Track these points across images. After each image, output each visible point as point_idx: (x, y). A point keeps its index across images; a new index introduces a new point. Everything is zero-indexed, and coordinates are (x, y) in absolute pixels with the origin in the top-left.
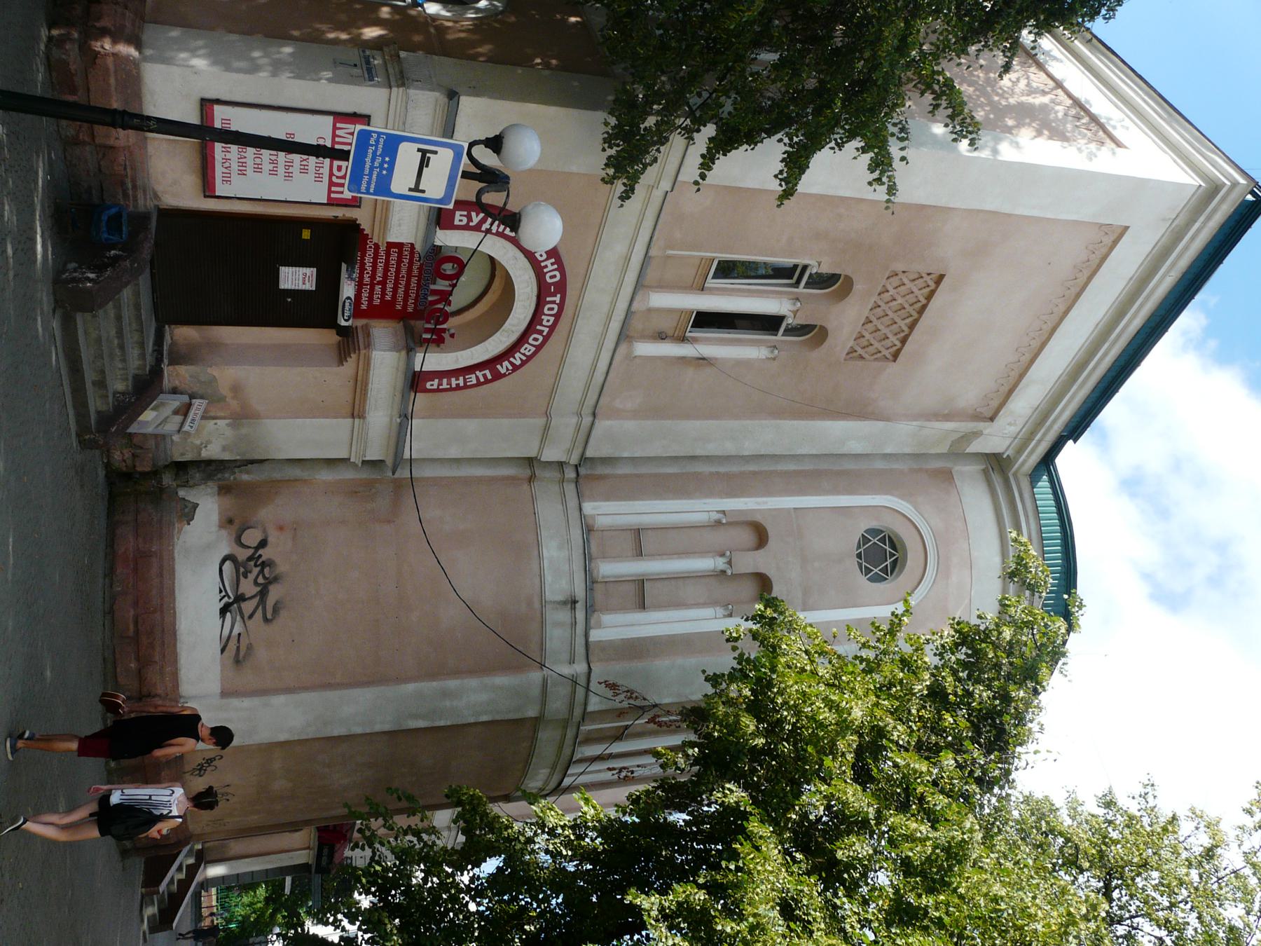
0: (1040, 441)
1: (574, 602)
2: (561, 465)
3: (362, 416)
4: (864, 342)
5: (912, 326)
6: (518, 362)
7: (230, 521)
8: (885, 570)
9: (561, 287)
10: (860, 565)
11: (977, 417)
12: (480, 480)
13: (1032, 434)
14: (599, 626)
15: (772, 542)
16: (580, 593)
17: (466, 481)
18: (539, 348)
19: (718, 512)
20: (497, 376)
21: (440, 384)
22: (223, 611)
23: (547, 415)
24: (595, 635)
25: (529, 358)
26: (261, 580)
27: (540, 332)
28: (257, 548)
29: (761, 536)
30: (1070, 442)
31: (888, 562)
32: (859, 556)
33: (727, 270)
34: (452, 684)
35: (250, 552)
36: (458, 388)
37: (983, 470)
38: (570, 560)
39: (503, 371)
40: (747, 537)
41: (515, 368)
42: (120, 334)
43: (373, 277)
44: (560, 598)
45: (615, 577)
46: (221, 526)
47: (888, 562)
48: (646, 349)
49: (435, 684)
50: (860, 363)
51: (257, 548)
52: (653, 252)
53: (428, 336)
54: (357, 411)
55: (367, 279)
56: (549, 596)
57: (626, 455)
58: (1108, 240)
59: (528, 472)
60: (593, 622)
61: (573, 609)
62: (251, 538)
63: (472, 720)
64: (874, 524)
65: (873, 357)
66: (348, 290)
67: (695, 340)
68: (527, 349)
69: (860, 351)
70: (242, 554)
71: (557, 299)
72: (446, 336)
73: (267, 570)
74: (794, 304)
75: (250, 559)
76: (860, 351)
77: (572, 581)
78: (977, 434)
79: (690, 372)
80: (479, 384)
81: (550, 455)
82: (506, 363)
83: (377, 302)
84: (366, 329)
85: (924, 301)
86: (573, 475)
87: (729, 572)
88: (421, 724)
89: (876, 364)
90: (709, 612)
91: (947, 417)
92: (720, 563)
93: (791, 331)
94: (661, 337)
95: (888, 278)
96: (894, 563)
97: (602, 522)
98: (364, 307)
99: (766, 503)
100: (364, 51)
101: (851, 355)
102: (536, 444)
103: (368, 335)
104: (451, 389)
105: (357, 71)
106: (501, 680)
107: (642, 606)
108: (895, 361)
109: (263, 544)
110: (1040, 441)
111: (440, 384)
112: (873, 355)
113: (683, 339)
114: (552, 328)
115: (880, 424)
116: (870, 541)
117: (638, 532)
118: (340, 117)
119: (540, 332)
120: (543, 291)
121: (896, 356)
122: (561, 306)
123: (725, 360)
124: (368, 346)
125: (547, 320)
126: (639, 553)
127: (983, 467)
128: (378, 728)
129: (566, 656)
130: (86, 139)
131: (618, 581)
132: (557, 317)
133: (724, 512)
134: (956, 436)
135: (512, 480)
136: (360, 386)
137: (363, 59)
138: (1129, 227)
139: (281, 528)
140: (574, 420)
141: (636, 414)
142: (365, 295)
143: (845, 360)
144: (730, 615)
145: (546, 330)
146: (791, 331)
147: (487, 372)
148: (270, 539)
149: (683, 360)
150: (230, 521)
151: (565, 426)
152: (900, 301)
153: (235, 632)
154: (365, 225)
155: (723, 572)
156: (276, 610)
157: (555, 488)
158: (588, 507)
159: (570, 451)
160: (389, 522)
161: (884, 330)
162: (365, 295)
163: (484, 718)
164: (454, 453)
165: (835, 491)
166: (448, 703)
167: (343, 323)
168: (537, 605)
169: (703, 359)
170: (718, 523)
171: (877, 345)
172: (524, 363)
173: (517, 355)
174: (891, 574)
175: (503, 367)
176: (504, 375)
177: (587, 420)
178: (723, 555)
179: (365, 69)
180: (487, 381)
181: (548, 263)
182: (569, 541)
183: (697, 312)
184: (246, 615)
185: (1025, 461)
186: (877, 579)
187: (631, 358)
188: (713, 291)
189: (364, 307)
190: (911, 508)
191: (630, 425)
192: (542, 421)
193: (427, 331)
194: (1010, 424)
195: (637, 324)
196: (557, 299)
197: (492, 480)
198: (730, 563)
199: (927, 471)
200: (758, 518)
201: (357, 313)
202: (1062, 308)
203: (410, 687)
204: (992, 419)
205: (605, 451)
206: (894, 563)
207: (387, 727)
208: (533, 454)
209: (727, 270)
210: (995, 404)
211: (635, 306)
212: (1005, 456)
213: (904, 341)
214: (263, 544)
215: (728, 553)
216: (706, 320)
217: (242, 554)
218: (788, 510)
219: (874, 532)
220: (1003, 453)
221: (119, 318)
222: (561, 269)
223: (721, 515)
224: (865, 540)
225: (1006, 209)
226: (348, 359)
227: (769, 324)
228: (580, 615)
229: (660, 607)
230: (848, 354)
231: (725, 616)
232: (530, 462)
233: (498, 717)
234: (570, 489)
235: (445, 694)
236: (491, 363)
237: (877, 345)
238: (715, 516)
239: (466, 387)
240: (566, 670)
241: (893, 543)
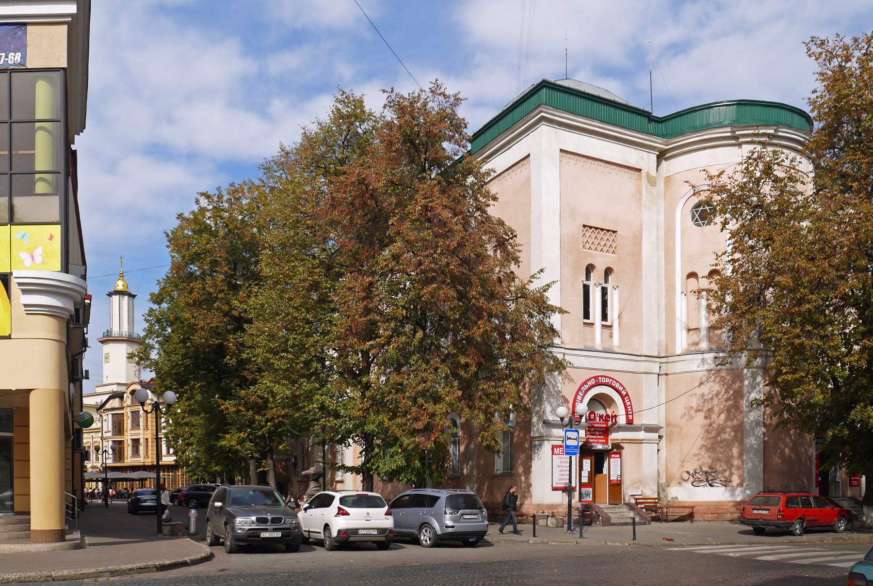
3: (642, 440)
5: (602, 230)
6: (622, 388)
7: (680, 483)
9: (596, 378)
18: (617, 382)
20: (627, 395)
21: (630, 414)
22: (711, 486)
25: (620, 384)
26: (701, 473)
27: (611, 382)
28: (690, 474)
29: (692, 275)
33: (586, 315)
35: (691, 477)
36: (631, 408)
39: (625, 393)
40: (692, 280)
41: (624, 389)
42: (616, 513)
43: (595, 439)
46: (682, 486)
47: (707, 208)
48: (616, 340)
50: (618, 247)
51: (690, 474)
52: (582, 347)
53: (614, 421)
54: (640, 442)
55: (596, 441)
62: (686, 476)
66: (600, 447)
68: (617, 385)
70: (691, 479)
71: (600, 378)
72: (613, 414)
73: (697, 471)
75: (693, 477)
78: (648, 174)
79: (624, 320)
80: (630, 401)
82: (623, 392)
83: (602, 437)
89: (618, 240)
91: (641, 194)
93: (606, 281)
94: (611, 336)
98: (605, 441)
103: (614, 440)
104: (632, 411)
108: (616, 232)
109: (688, 472)
111: (630, 414)
113: (611, 327)
114: (610, 378)
115: (644, 227)
118: (553, 453)
119: (611, 382)
120: (598, 384)
121: (614, 232)
122: (602, 376)
123: (620, 308)
125: (607, 380)
132: (606, 377)
133: (682, 292)
134: (649, 185)
139: (683, 466)
142: (601, 441)
145: (611, 380)
146: (606, 281)
147: (626, 399)
148: (687, 470)
149: (619, 324)
150: (680, 483)
151: (643, 366)
153: (720, 482)
156: (713, 469)
158: (678, 352)
160: (681, 429)
162: (601, 441)
165: (674, 239)
167: (610, 448)
170: (685, 295)
172: (622, 386)
173: (619, 389)
175: (624, 393)
176: (627, 392)
177: (643, 358)
180: (629, 398)
181: (589, 384)
182: (690, 360)
183: (602, 320)
184: (713, 478)
187: (619, 347)
188: (594, 319)
189: (605, 441)
193: (612, 421)
195: (607, 346)
196: (600, 378)
199: (665, 191)
201: (607, 443)
204: (640, 170)
209: (586, 315)
211: (601, 349)
212: (658, 153)
214: (688, 472)
216: (604, 317)
217: (691, 479)
218: (682, 262)
219: (693, 217)
222: (590, 379)
223: (683, 294)
227: (604, 291)
234: (670, 359)
236: (623, 398)
239: (631, 405)
241: (698, 206)
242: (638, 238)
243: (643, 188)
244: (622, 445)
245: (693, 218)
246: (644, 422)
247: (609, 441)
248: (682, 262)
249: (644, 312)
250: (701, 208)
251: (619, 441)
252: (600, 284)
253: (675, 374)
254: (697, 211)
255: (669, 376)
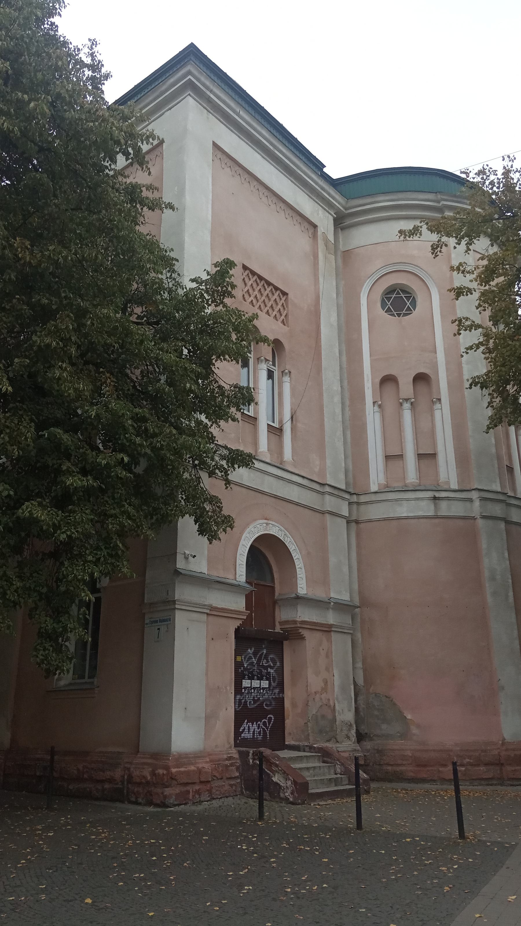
0: (329, 194)
1: (435, 498)
2: (350, 504)
3: (331, 626)
4: (278, 315)
5: (269, 284)
8: (408, 298)
10: (405, 315)
11: (315, 236)
12: (359, 554)
13: (323, 199)
14: (448, 483)
15: (393, 373)
16: (430, 494)
17: (359, 562)
19: (374, 406)
23: (323, 513)
24: (454, 485)
30: (325, 170)
31: (403, 296)
32: (399, 315)
34: (486, 574)
37: (341, 229)
38: (408, 500)
40: (389, 388)
44: (432, 507)
45: (417, 472)
47: (403, 296)
48: (288, 454)
49: (487, 585)
56: (431, 513)
57: (343, 465)
58: (220, 155)
59: (353, 524)
60: (446, 487)
61: (439, 499)
63: (508, 562)
64: (379, 305)
65: (286, 309)
67: (281, 422)
69: (283, 317)
74: (262, 361)
76: (283, 317)
77: (422, 499)
81: (345, 512)
84: (281, 623)
85: (256, 277)
86: (355, 496)
87: (413, 400)
88: (511, 594)
89: (290, 306)
90: (437, 414)
91: (316, 257)
92: (407, 405)
95: (245, 301)
96: (404, 291)
97: (382, 480)
99: (368, 375)
100: (147, 624)
101: (285, 322)
102: (339, 520)
103: (287, 622)
105: (163, 629)
106: (484, 544)
107: (433, 456)
108: (287, 294)
110: (329, 194)
112: (284, 309)
116: (389, 307)
117: (388, 458)
121: (285, 294)
123: (292, 404)
124: (295, 622)
126: (401, 457)
127: (340, 230)
128: (514, 620)
129: (468, 504)
130: (209, 786)
131: (419, 470)
133: (374, 403)
135: (358, 535)
136: (315, 627)
137: (154, 624)
138: (213, 142)
140: (327, 497)
141: (323, 458)
143: (288, 327)
144: (439, 400)
149: (293, 429)
152: (256, 292)
154: (238, 623)
155: (412, 404)
157: (362, 508)
158: (374, 488)
159: (343, 499)
161: (272, 302)
163: (506, 555)
164: (346, 569)
166: (498, 577)
168: (437, 521)
169: (292, 418)
170: (380, 406)
171: (279, 306)
174: (411, 294)
177: (327, 489)
178: (401, 404)
179: (161, 624)
182: (396, 500)
185: (339, 203)
186: (414, 303)
190: (368, 281)
191: (328, 462)
192: (327, 515)
194: (318, 214)
197: (358, 546)
198: (407, 400)
200: (378, 380)
202: (255, 183)
203: (490, 599)
204: (315, 226)
205: (342, 476)
206: (404, 291)
207: (514, 615)
208: (344, 521)
210: (306, 224)
212: (335, 216)
213: (277, 289)
215: (401, 401)
219: (383, 305)
220: (334, 217)
221: (308, 769)
223: (376, 405)
224: (388, 311)
225: (209, 225)
226: (302, 634)
228: (443, 494)
229: (434, 444)
230: (284, 325)
231: (440, 403)
232: (348, 522)
233: (505, 547)
234: (363, 499)
235: (493, 578)
237: (279, 306)
238: (376, 408)
240: (477, 503)
241: (390, 291)
242: (316, 314)
243: (319, 250)
244: (305, 633)
245: (383, 308)
246: (332, 595)
247: (277, 624)
248: (373, 362)
249: (326, 420)
250: (394, 295)
251: (299, 625)
252: (266, 360)
253: (370, 521)
254: (389, 299)
255: (362, 526)
